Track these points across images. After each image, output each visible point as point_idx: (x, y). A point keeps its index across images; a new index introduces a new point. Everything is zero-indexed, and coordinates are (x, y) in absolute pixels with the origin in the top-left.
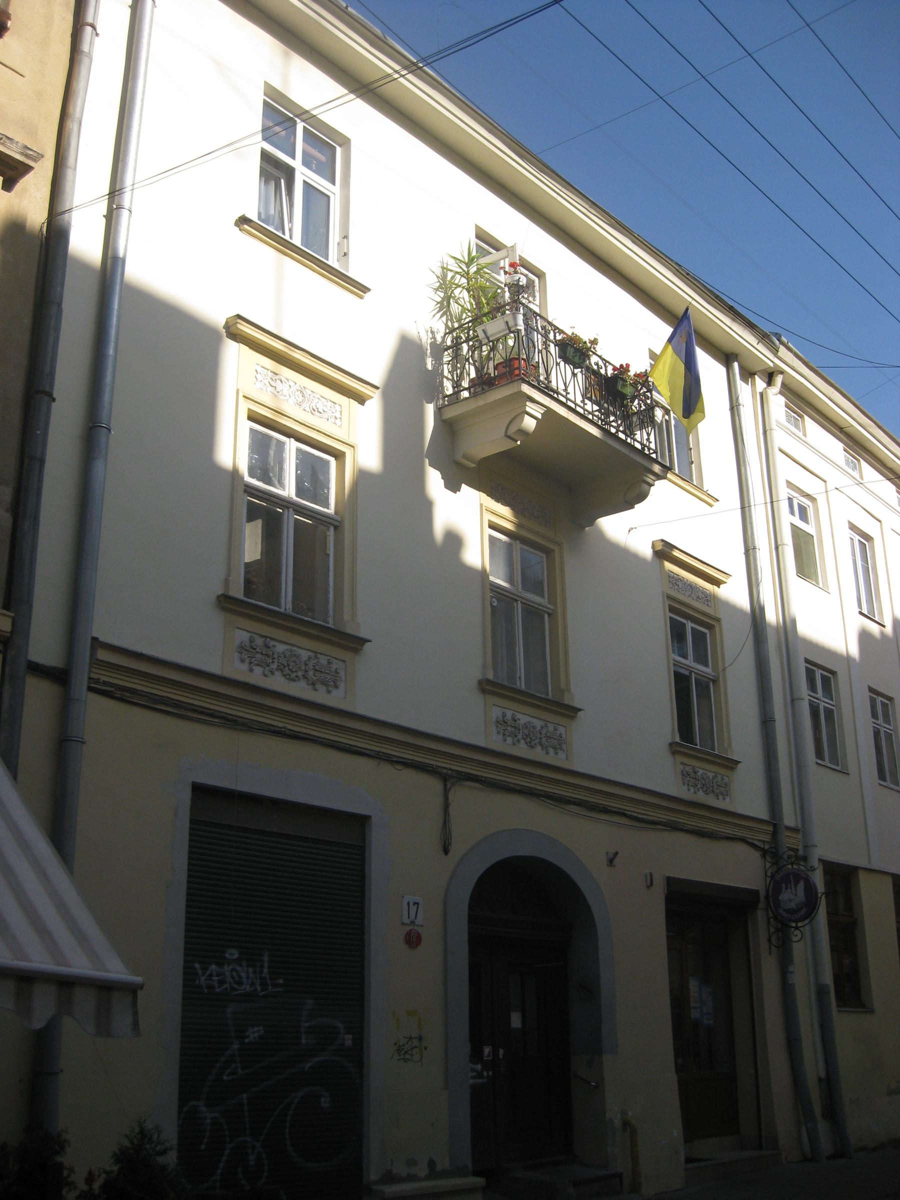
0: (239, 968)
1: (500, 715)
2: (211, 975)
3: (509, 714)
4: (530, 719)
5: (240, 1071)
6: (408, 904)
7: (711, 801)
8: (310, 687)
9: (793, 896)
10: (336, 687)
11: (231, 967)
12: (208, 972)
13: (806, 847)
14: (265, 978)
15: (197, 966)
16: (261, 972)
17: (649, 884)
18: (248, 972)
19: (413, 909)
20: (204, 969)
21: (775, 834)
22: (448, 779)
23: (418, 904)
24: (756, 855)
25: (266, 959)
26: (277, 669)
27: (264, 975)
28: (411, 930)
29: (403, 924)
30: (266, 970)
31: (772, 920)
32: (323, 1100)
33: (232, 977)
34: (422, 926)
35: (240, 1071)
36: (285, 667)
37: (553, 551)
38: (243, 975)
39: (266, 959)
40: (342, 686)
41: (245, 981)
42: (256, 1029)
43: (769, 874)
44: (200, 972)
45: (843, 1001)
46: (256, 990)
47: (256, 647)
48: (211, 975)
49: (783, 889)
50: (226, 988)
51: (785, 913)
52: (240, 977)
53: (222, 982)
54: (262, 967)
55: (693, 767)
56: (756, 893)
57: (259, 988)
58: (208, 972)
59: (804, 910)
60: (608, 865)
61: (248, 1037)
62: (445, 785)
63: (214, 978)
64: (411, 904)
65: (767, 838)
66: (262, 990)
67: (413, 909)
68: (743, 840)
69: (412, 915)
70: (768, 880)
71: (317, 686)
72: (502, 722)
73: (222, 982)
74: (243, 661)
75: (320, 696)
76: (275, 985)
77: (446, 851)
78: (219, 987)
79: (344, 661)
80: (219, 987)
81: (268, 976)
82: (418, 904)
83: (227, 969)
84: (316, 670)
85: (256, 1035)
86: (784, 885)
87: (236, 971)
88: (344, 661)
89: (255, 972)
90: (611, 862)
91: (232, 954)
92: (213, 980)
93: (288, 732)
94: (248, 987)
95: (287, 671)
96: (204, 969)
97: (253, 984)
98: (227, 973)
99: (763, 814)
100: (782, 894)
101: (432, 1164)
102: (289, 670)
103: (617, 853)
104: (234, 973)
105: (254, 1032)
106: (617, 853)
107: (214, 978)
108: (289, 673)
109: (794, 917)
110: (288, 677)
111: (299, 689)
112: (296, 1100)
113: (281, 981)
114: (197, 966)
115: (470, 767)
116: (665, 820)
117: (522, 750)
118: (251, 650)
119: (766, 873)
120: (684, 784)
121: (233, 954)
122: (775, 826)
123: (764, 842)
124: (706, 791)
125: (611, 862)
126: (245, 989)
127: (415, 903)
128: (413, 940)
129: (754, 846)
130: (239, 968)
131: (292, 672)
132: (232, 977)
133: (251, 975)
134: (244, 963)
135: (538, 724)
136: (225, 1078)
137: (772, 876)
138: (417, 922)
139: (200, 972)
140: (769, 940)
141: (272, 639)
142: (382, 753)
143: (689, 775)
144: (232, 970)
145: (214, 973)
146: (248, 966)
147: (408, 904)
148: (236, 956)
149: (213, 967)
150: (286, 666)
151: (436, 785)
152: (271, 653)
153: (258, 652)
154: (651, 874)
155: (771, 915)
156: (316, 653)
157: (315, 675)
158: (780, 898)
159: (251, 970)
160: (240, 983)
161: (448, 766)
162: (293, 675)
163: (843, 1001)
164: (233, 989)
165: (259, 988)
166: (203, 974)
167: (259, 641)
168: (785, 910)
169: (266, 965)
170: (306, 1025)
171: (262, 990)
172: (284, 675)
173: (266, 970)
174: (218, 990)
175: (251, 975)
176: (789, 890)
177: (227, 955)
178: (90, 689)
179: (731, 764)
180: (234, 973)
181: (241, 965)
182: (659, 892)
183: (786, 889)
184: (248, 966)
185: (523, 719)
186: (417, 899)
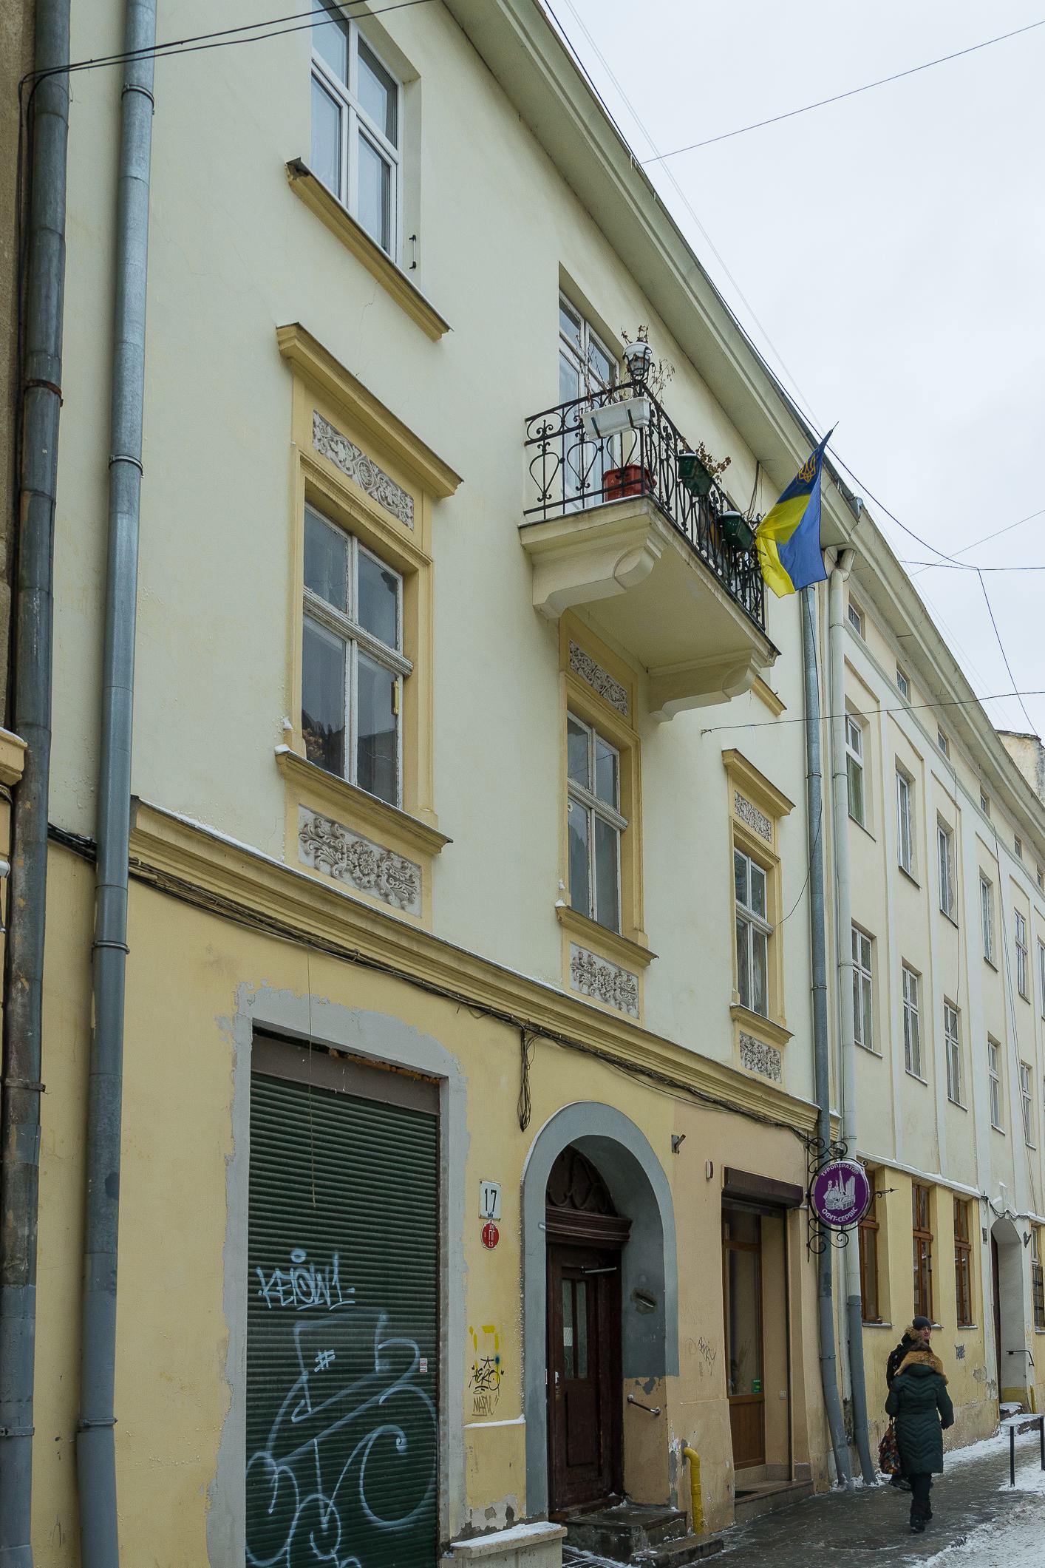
0: (306, 1275)
1: (576, 954)
2: (275, 1284)
5: (310, 1409)
6: (486, 1192)
7: (763, 1078)
8: (381, 898)
9: (840, 1196)
10: (411, 901)
11: (297, 1274)
12: (272, 1281)
13: (843, 1141)
14: (335, 1287)
16: (331, 1280)
17: (709, 1176)
18: (316, 1280)
20: (268, 1276)
21: (818, 1123)
22: (528, 1033)
23: (495, 1192)
24: (800, 1146)
25: (336, 1261)
26: (346, 870)
27: (333, 1284)
28: (488, 1225)
29: (481, 1217)
30: (336, 1277)
31: (812, 1223)
32: (398, 1440)
33: (300, 1286)
35: (310, 1409)
36: (355, 867)
37: (628, 748)
38: (312, 1284)
39: (336, 1261)
40: (417, 901)
41: (313, 1291)
42: (326, 1354)
43: (812, 1169)
44: (263, 1280)
45: (865, 1318)
46: (325, 1303)
47: (322, 835)
48: (275, 1284)
49: (830, 1187)
50: (293, 1302)
51: (830, 1214)
52: (308, 1286)
53: (288, 1293)
54: (332, 1272)
55: (751, 1038)
56: (800, 1189)
57: (328, 1300)
58: (272, 1281)
59: (854, 1211)
62: (522, 1041)
63: (278, 1288)
64: (489, 1192)
65: (810, 1127)
66: (333, 1303)
68: (790, 1128)
69: (490, 1210)
70: (811, 1175)
71: (390, 897)
72: (578, 966)
73: (288, 1293)
74: (307, 854)
75: (392, 911)
76: (345, 1296)
78: (285, 1300)
79: (419, 867)
80: (285, 1300)
81: (338, 1285)
82: (495, 1192)
83: (293, 1276)
84: (390, 876)
85: (327, 1361)
86: (830, 1182)
87: (304, 1279)
88: (419, 867)
89: (324, 1279)
90: (675, 1147)
91: (298, 1256)
92: (278, 1291)
94: (316, 1299)
95: (357, 873)
96: (268, 1276)
97: (322, 1295)
98: (294, 1282)
99: (807, 1097)
100: (828, 1192)
101: (510, 1513)
102: (358, 870)
103: (684, 1136)
104: (301, 1282)
105: (324, 1359)
106: (684, 1136)
107: (278, 1288)
108: (361, 875)
109: (841, 1219)
110: (358, 881)
111: (370, 899)
112: (371, 1443)
113: (352, 1291)
115: (547, 1020)
116: (723, 1100)
118: (315, 838)
119: (808, 1168)
120: (742, 1058)
121: (299, 1255)
122: (820, 1112)
123: (808, 1131)
124: (761, 1068)
125: (675, 1147)
126: (314, 1301)
127: (492, 1191)
128: (490, 1237)
129: (798, 1135)
130: (306, 1275)
131: (364, 875)
132: (300, 1286)
133: (320, 1283)
134: (312, 1268)
136: (294, 1419)
137: (816, 1172)
138: (496, 1215)
139: (263, 1280)
140: (808, 1245)
141: (341, 826)
142: (460, 995)
143: (747, 1047)
144: (300, 1277)
145: (279, 1281)
146: (316, 1271)
147: (486, 1192)
148: (303, 1259)
149: (278, 1273)
150: (356, 866)
151: (510, 1039)
152: (340, 845)
153: (325, 843)
154: (711, 1163)
155: (811, 1216)
156: (389, 852)
157: (387, 881)
158: (825, 1197)
159: (319, 1276)
160: (308, 1294)
161: (526, 1017)
162: (365, 879)
163: (865, 1318)
164: (300, 1302)
165: (328, 1300)
166: (267, 1283)
167: (326, 827)
168: (829, 1211)
169: (336, 1270)
170: (380, 1346)
171: (333, 1303)
172: (354, 879)
173: (336, 1277)
174: (283, 1305)
175: (320, 1283)
176: (837, 1188)
177: (293, 1258)
178: (132, 876)
179: (783, 1035)
180: (301, 1282)
181: (308, 1270)
182: (718, 1184)
183: (833, 1187)
184: (316, 1271)
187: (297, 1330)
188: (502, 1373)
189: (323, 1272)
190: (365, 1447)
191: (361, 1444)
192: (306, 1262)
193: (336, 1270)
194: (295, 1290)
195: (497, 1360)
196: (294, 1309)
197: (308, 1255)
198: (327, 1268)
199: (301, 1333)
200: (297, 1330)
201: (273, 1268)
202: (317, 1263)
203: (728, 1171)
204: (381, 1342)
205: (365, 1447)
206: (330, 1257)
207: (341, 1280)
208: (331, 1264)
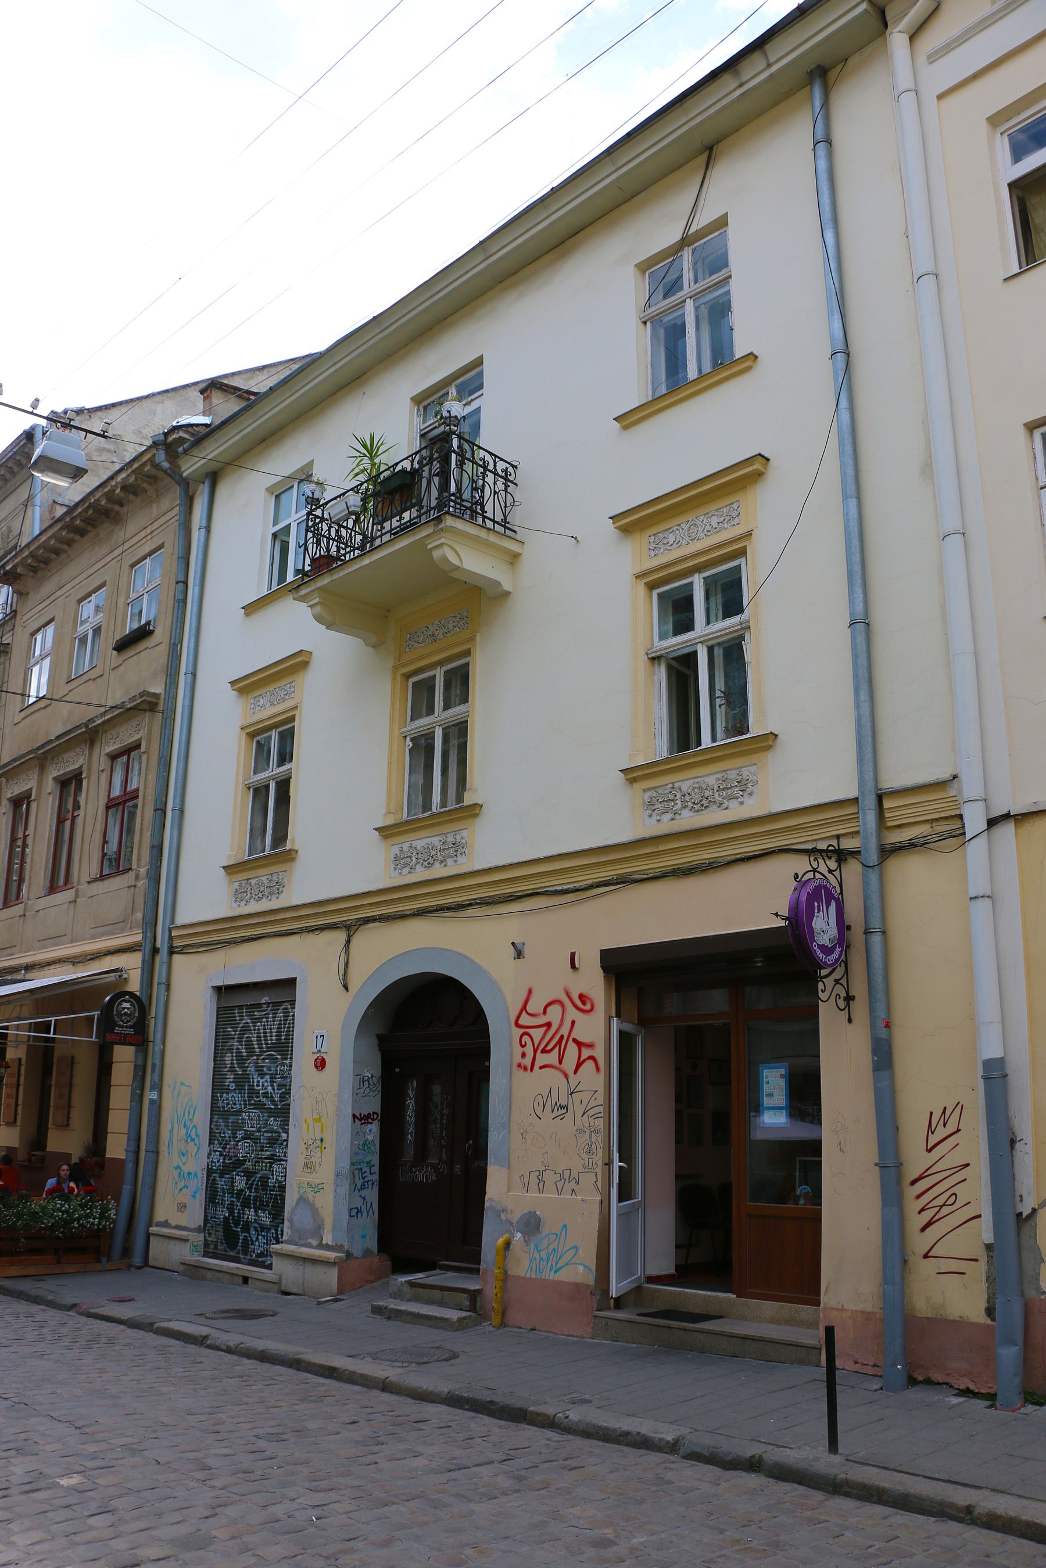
0: (235, 1095)
3: (406, 846)
4: (428, 840)
15: (219, 1095)
19: (320, 1040)
23: (323, 1036)
29: (313, 1053)
30: (246, 1095)
34: (326, 1053)
38: (237, 1099)
48: (224, 1100)
53: (228, 1104)
54: (245, 1093)
60: (515, 959)
61: (237, 1137)
64: (319, 1037)
67: (320, 1040)
73: (228, 1104)
76: (250, 1105)
77: (346, 987)
82: (323, 1036)
83: (230, 1095)
93: (254, 937)
113: (253, 1102)
114: (219, 1095)
115: (366, 911)
117: (421, 874)
127: (321, 1036)
128: (320, 1064)
130: (235, 1095)
135: (436, 841)
136: (227, 1161)
144: (233, 1096)
149: (225, 1095)
151: (341, 936)
164: (232, 1108)
169: (246, 1092)
177: (230, 1088)
184: (239, 1093)
185: (420, 844)
186: (323, 1032)
187: (230, 1121)
188: (325, 1148)
189: (241, 1093)
190: (254, 1181)
191: (253, 1179)
192: (235, 1089)
193: (246, 1092)
194: (231, 1102)
195: (322, 1140)
196: (230, 1111)
197: (236, 1086)
198: (243, 1091)
199: (232, 1122)
200: (230, 1121)
201: (223, 1093)
202: (239, 1089)
203: (605, 955)
204: (264, 1128)
205: (254, 1181)
206: (244, 1086)
207: (248, 1097)
208: (245, 1089)
